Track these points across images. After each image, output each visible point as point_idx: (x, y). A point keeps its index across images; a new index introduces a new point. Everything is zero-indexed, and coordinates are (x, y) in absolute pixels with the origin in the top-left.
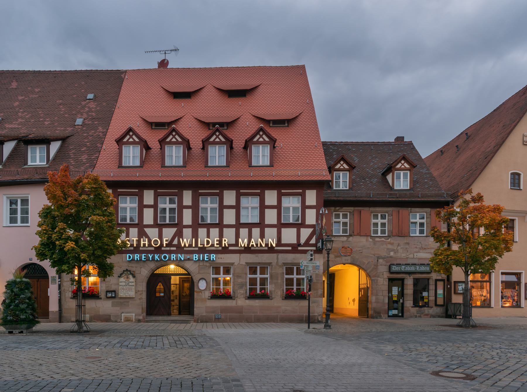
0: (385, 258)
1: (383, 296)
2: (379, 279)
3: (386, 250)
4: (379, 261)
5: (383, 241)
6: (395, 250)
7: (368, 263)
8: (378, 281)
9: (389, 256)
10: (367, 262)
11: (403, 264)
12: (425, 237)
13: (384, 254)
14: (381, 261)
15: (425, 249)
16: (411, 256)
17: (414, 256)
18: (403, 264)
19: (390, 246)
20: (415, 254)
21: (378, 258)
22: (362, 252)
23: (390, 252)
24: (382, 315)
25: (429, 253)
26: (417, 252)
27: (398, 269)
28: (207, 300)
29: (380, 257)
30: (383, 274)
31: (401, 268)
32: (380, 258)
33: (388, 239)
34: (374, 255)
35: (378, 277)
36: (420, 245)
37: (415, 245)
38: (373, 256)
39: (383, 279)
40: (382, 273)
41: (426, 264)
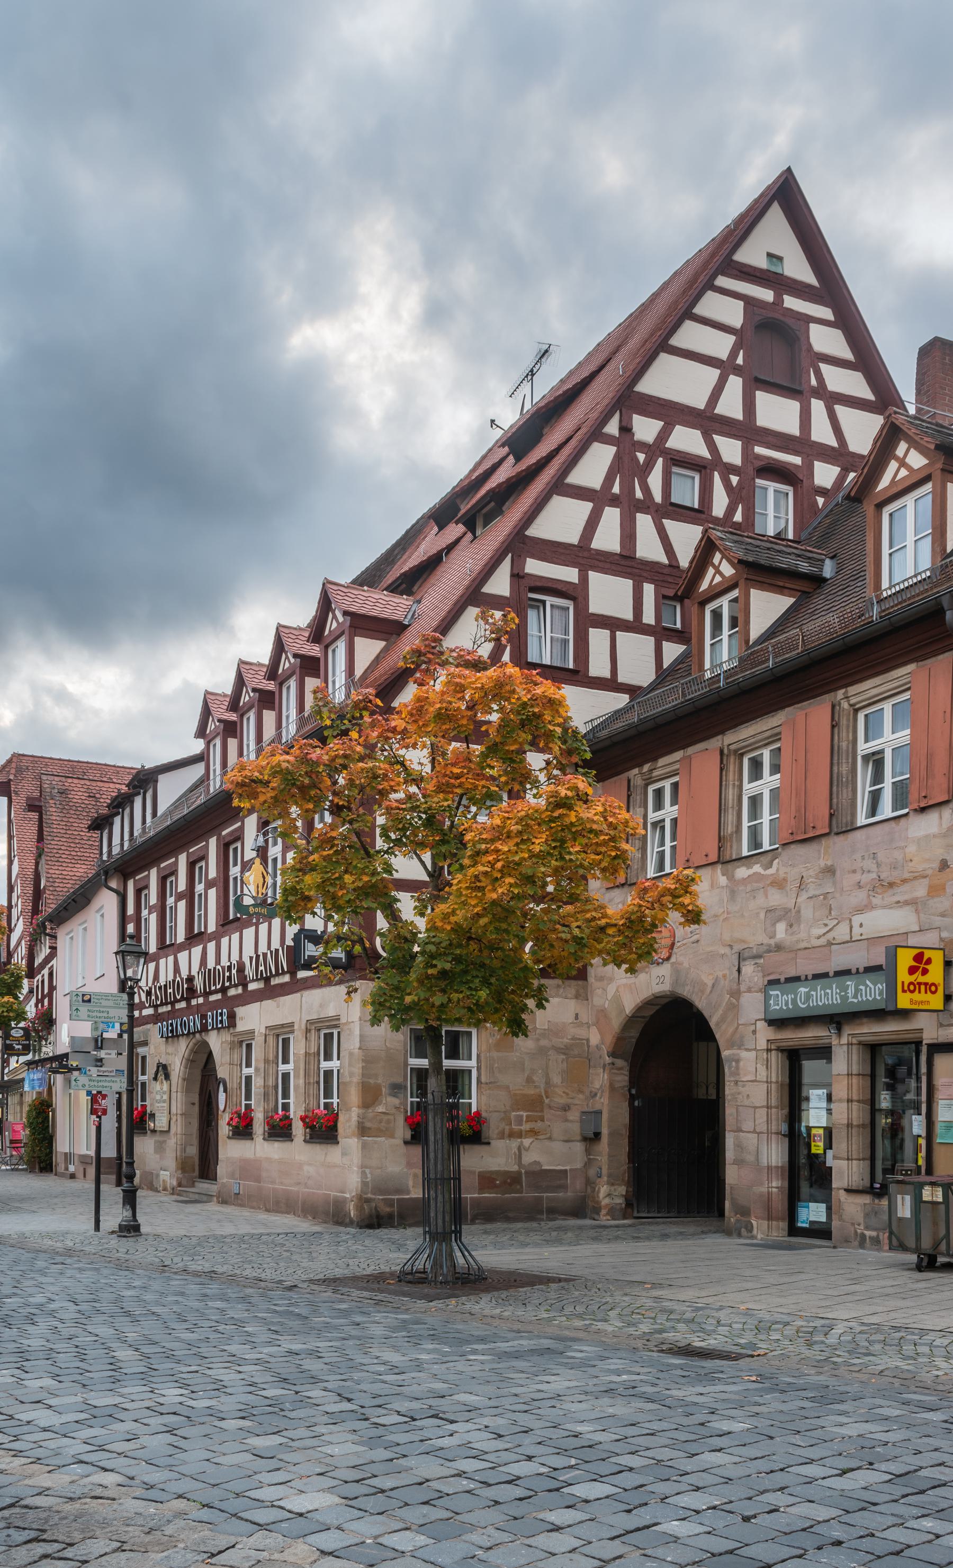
0: (760, 957)
1: (754, 1132)
2: (744, 1054)
3: (762, 915)
4: (744, 970)
5: (756, 877)
6: (790, 910)
7: (713, 985)
8: (741, 1064)
9: (772, 942)
10: (710, 983)
11: (858, 972)
12: (893, 824)
13: (756, 938)
14: (748, 969)
15: (891, 885)
16: (841, 933)
17: (851, 928)
18: (858, 972)
19: (776, 898)
20: (856, 920)
21: (741, 958)
22: (698, 941)
23: (774, 925)
24: (754, 1223)
25: (907, 903)
26: (860, 910)
27: (787, 1004)
28: (228, 1141)
29: (746, 954)
30: (754, 1032)
31: (796, 997)
32: (744, 960)
33: (770, 865)
34: (731, 946)
35: (740, 1046)
36: (874, 867)
37: (854, 871)
38: (726, 950)
39: (754, 1053)
40: (753, 1028)
41: (782, 980)
